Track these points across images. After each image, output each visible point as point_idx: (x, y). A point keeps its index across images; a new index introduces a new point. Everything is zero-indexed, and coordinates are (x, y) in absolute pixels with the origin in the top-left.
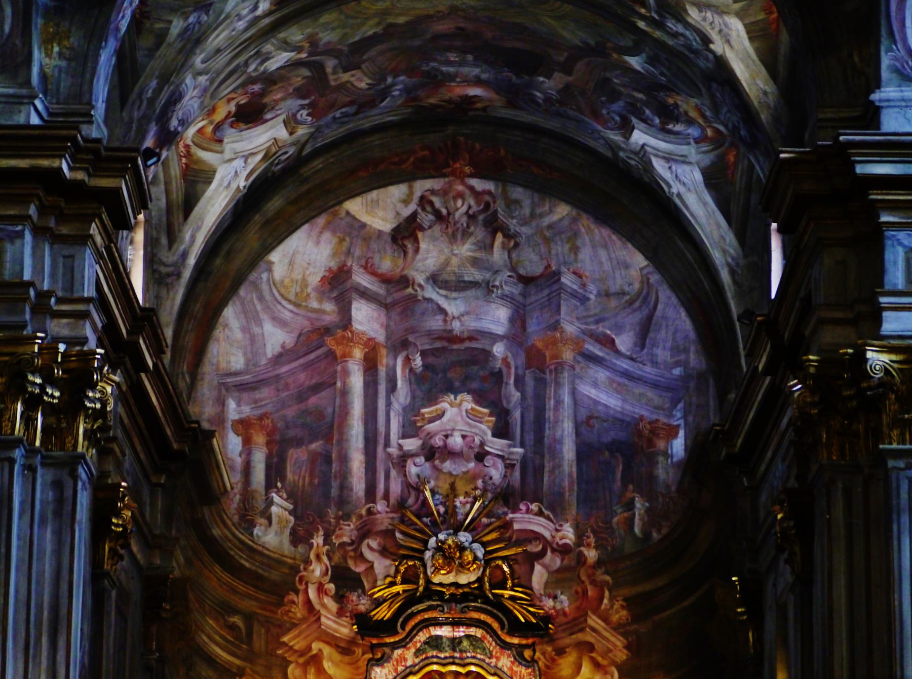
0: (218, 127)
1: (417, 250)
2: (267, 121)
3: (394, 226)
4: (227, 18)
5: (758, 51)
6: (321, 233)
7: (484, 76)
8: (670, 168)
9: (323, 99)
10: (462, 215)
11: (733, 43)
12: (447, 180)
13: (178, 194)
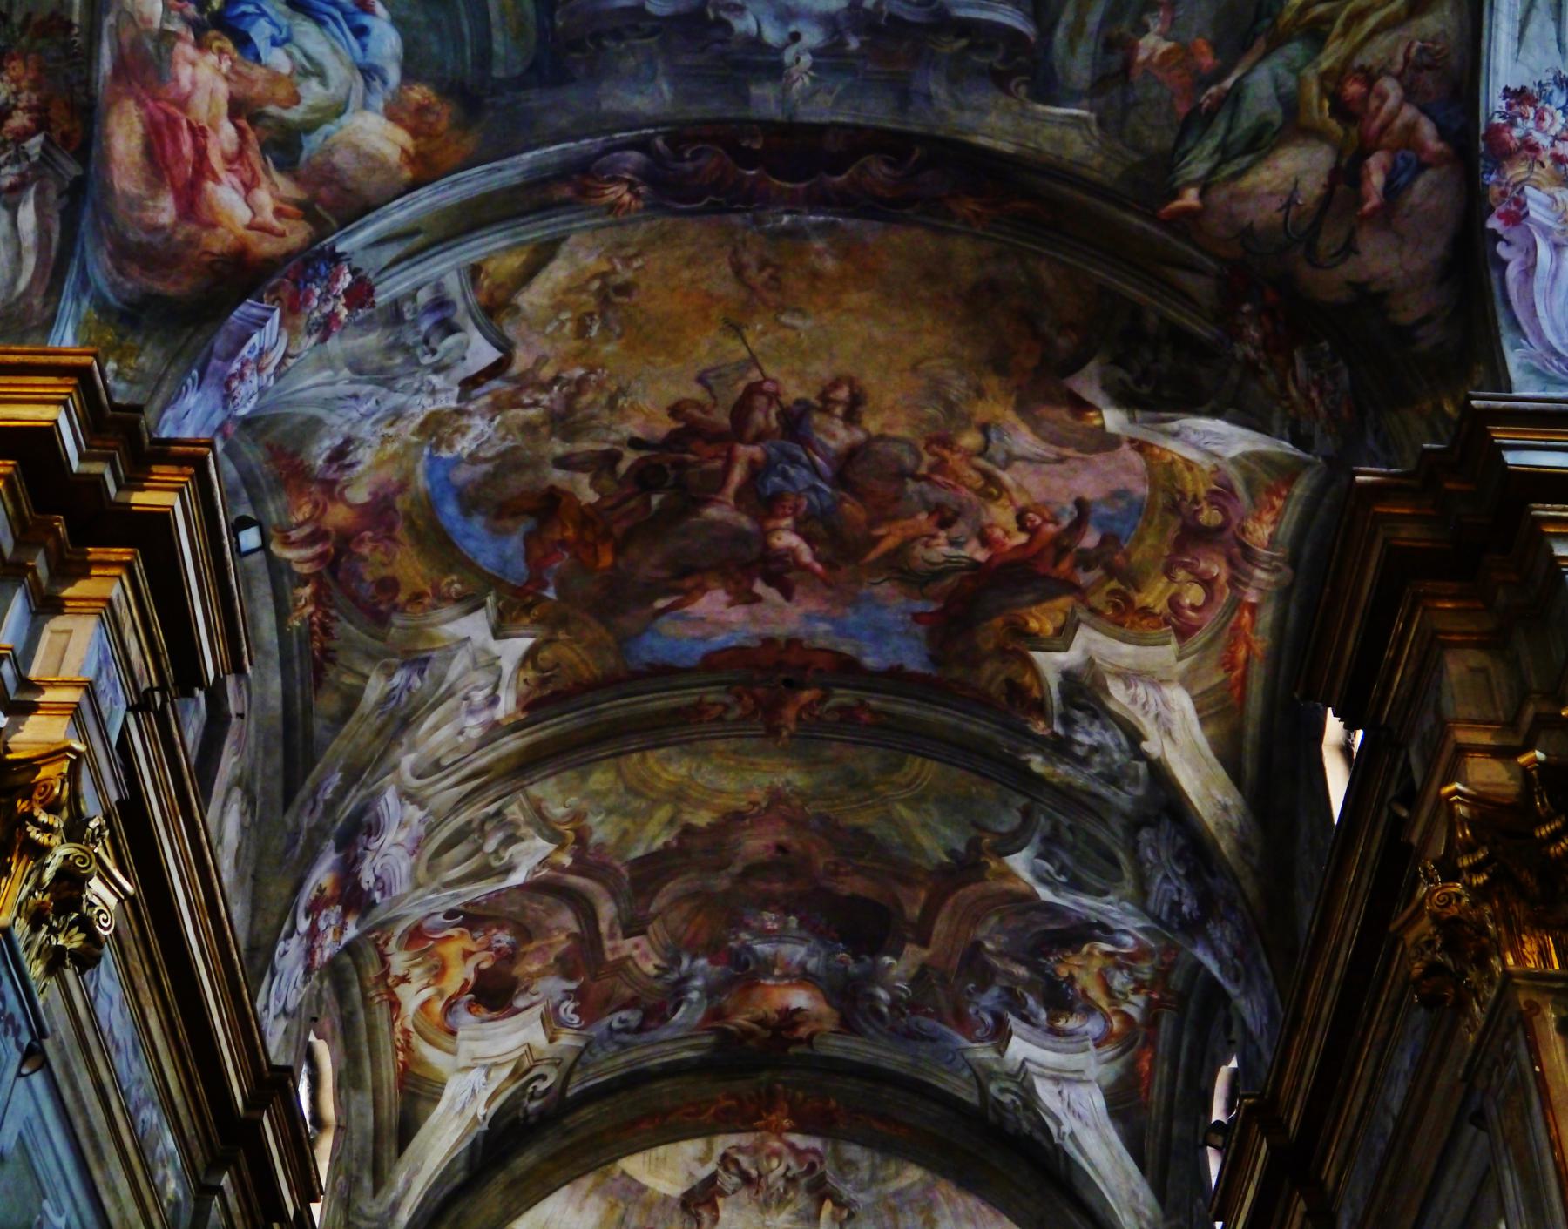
0: (449, 1007)
1: (715, 1220)
2: (518, 1011)
3: (685, 1189)
4: (450, 693)
5: (1212, 741)
6: (586, 1196)
7: (812, 964)
8: (1060, 1093)
9: (596, 984)
10: (777, 1179)
11: (1177, 734)
12: (758, 1134)
13: (390, 1114)
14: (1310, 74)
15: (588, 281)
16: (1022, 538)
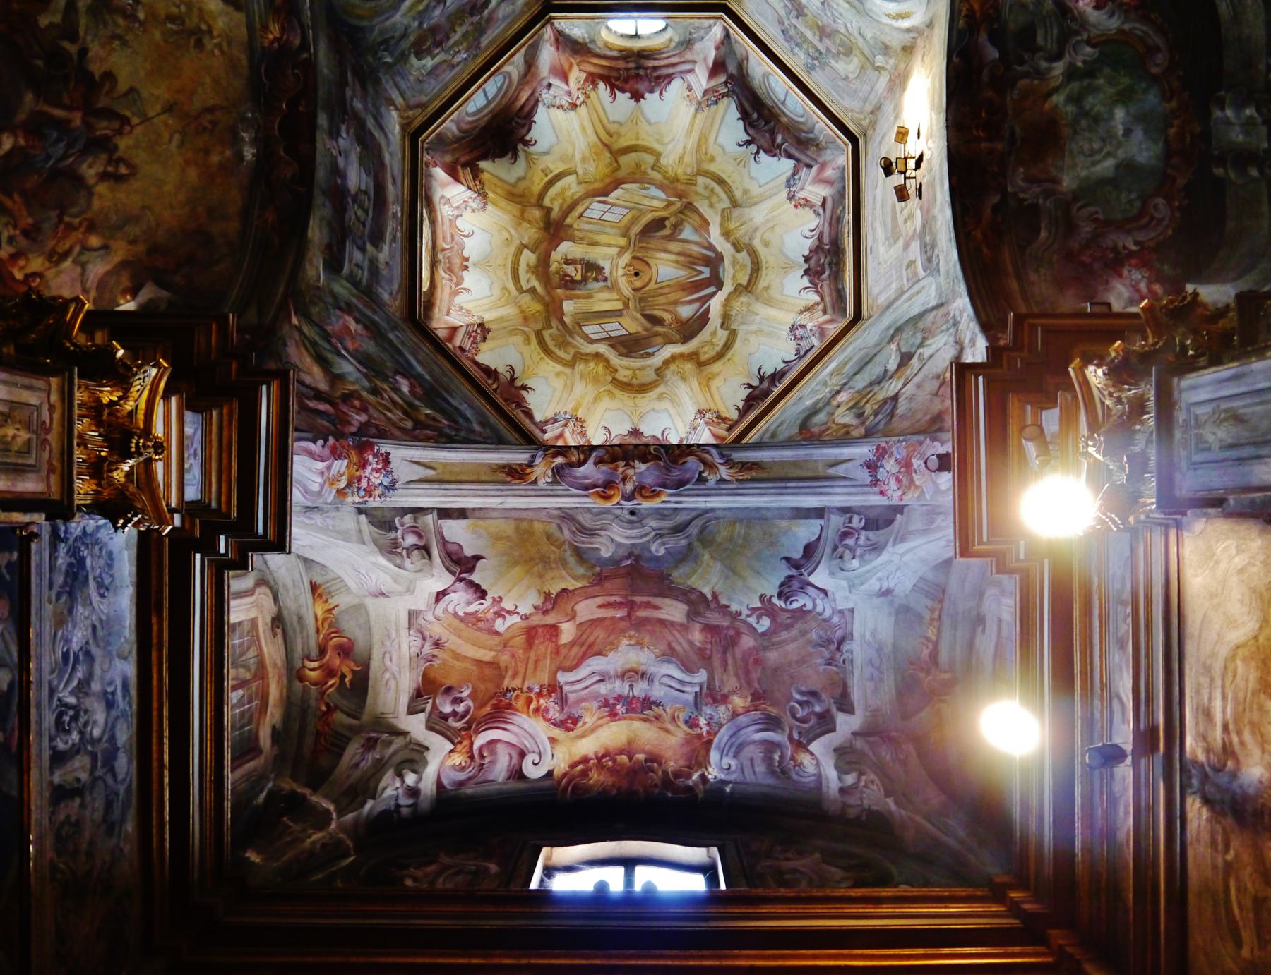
14: (357, 387)
15: (206, 22)
16: (19, 276)
